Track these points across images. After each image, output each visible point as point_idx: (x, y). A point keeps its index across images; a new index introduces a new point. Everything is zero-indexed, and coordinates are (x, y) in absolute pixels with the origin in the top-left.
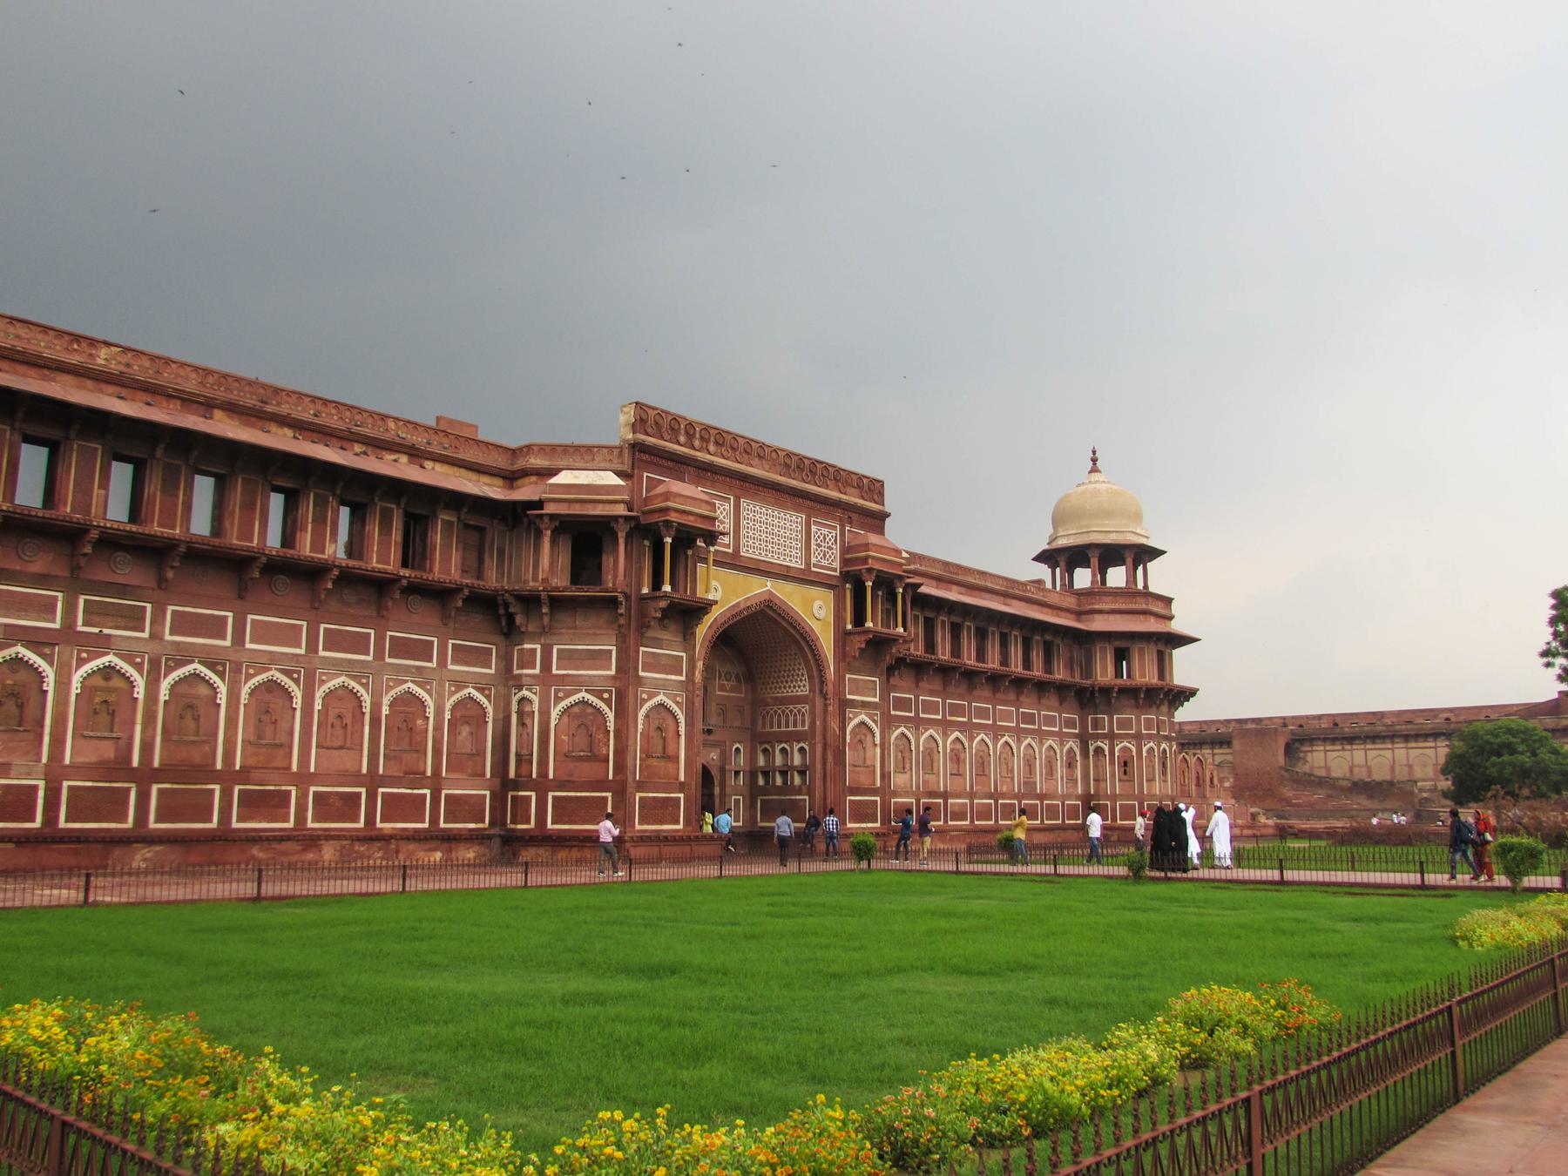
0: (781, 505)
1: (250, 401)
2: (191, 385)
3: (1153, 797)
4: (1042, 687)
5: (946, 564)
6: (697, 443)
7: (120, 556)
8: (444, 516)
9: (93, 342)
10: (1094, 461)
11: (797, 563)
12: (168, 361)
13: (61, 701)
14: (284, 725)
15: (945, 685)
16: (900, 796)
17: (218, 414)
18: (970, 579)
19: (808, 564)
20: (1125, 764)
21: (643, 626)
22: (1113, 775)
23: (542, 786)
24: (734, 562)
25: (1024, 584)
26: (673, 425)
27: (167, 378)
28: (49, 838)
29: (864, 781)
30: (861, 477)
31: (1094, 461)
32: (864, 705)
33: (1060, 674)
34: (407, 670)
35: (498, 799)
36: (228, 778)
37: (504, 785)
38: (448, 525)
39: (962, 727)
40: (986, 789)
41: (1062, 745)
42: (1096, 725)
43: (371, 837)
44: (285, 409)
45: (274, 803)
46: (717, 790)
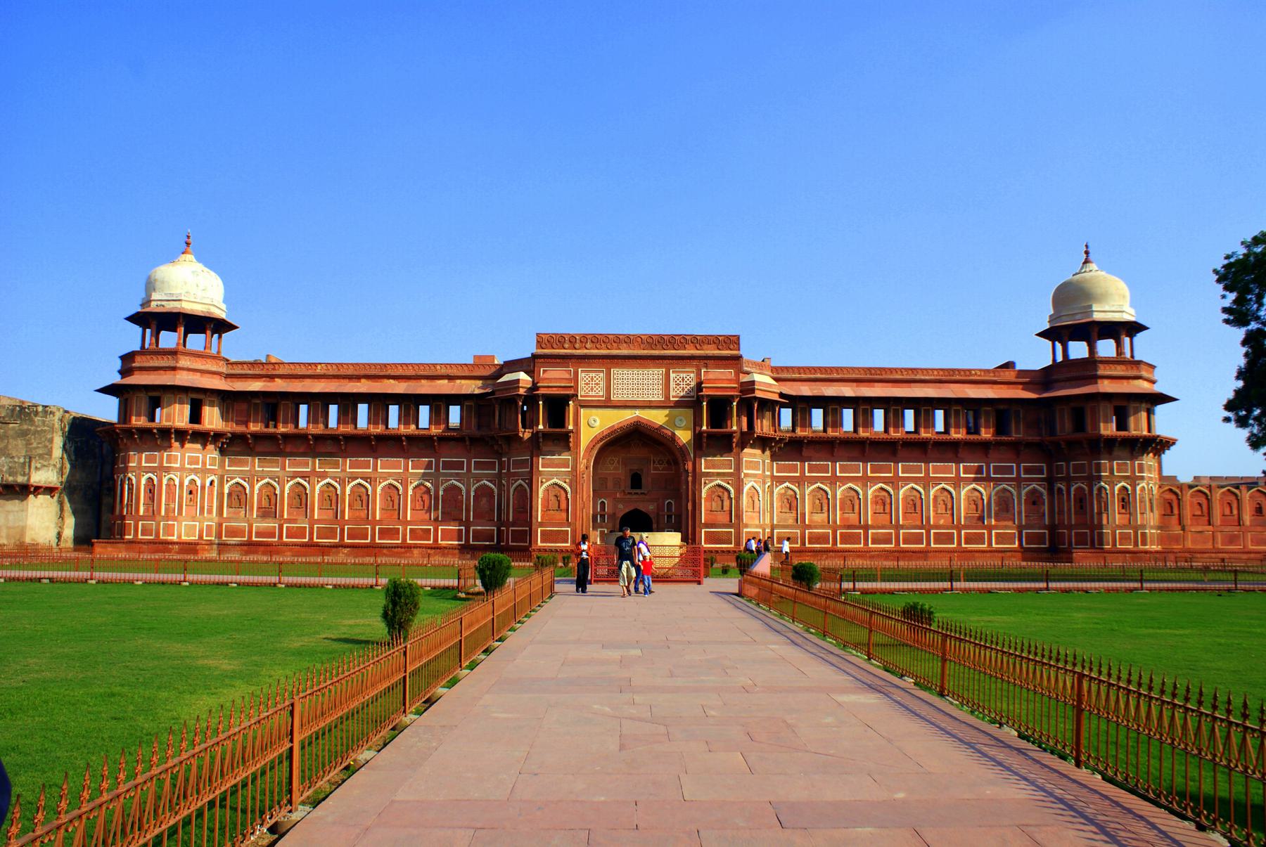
0: (646, 367)
1: (373, 372)
2: (350, 372)
3: (1100, 526)
4: (984, 448)
5: (869, 369)
6: (577, 346)
7: (329, 442)
8: (467, 403)
9: (316, 364)
10: (1087, 253)
11: (658, 397)
12: (341, 364)
13: (313, 497)
14: (396, 502)
15: (863, 452)
16: (816, 527)
17: (363, 381)
18: (898, 377)
19: (667, 396)
20: (1081, 500)
21: (538, 448)
22: (1069, 510)
23: (508, 524)
24: (607, 404)
25: (970, 370)
26: (560, 340)
27: (342, 372)
28: (310, 545)
29: (723, 518)
30: (717, 337)
31: (1087, 253)
32: (719, 474)
33: (1017, 434)
34: (451, 475)
35: (499, 531)
36: (374, 523)
37: (500, 523)
38: (469, 408)
39: (885, 480)
40: (919, 523)
41: (1019, 488)
42: (1059, 469)
43: (436, 547)
44: (390, 372)
45: (393, 533)
46: (655, 526)
